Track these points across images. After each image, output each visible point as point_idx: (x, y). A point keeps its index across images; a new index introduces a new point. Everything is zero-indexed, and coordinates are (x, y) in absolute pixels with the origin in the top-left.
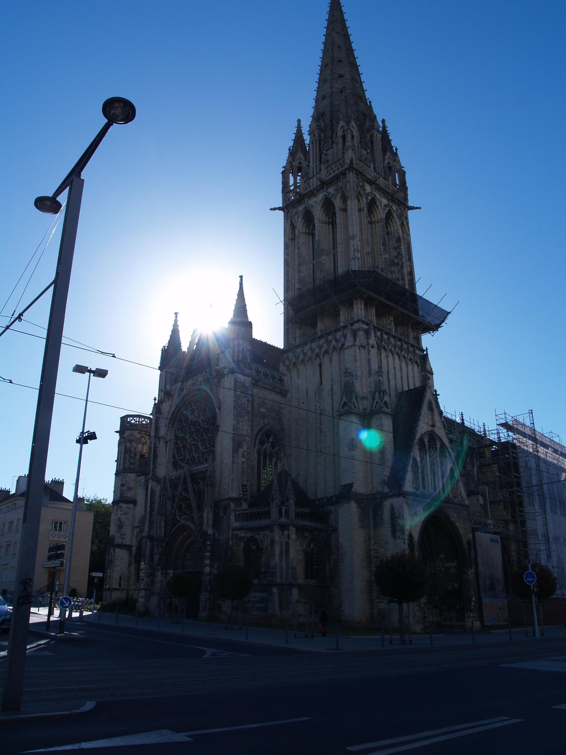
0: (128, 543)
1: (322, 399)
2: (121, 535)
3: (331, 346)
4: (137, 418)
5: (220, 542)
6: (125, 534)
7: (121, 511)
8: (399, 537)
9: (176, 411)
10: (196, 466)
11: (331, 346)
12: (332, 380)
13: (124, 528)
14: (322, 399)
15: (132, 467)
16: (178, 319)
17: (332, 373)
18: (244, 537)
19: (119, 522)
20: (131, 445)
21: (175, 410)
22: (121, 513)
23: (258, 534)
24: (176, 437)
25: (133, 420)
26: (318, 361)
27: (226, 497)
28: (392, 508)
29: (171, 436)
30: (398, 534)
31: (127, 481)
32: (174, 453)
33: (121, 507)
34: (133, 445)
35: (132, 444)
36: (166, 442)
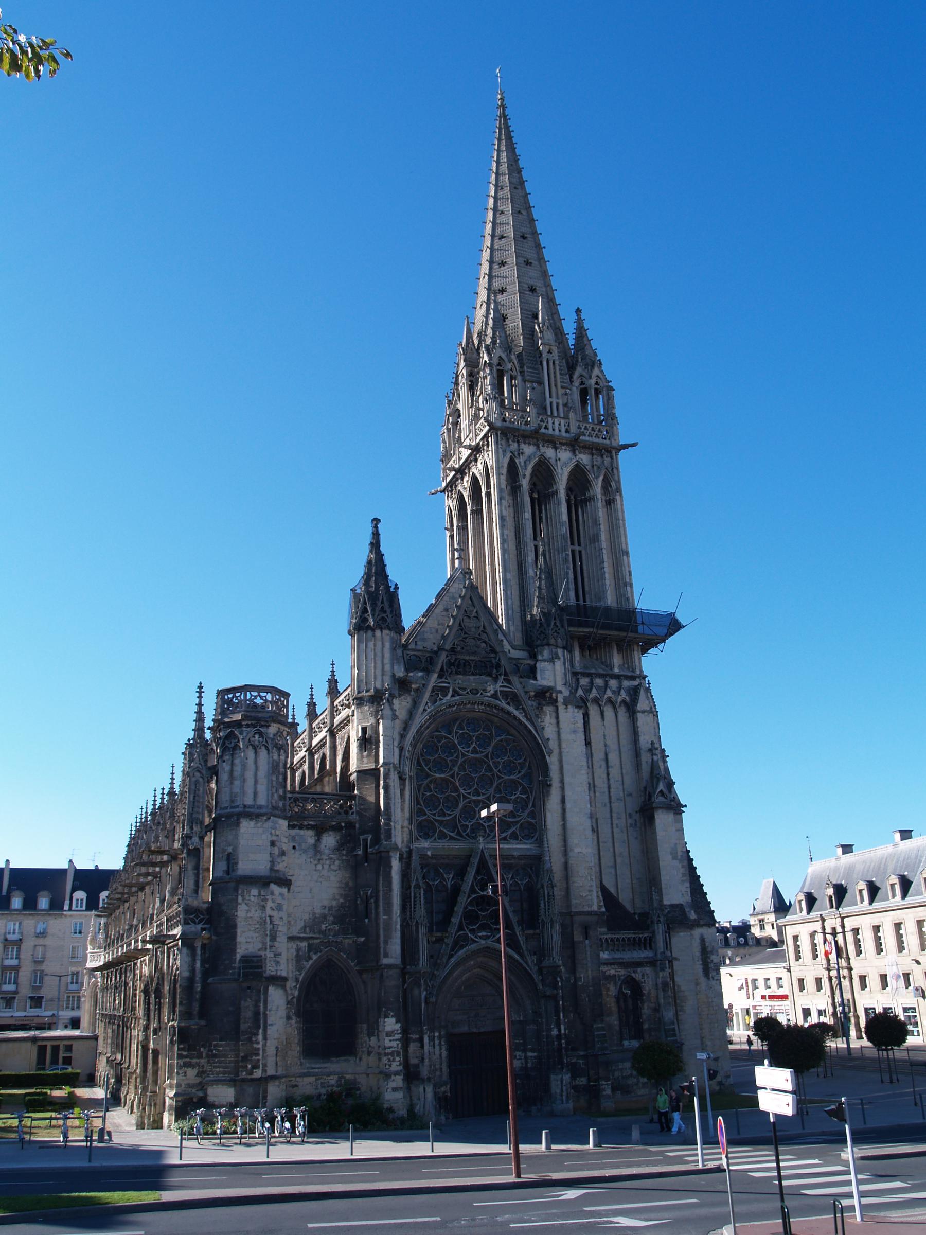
0: (284, 974)
5: (580, 983)
7: (273, 901)
8: (713, 978)
11: (606, 696)
12: (606, 745)
16: (380, 531)
17: (604, 736)
18: (615, 976)
23: (634, 972)
24: (421, 774)
27: (587, 909)
28: (703, 940)
30: (713, 974)
32: (418, 803)
33: (272, 893)
36: (402, 779)
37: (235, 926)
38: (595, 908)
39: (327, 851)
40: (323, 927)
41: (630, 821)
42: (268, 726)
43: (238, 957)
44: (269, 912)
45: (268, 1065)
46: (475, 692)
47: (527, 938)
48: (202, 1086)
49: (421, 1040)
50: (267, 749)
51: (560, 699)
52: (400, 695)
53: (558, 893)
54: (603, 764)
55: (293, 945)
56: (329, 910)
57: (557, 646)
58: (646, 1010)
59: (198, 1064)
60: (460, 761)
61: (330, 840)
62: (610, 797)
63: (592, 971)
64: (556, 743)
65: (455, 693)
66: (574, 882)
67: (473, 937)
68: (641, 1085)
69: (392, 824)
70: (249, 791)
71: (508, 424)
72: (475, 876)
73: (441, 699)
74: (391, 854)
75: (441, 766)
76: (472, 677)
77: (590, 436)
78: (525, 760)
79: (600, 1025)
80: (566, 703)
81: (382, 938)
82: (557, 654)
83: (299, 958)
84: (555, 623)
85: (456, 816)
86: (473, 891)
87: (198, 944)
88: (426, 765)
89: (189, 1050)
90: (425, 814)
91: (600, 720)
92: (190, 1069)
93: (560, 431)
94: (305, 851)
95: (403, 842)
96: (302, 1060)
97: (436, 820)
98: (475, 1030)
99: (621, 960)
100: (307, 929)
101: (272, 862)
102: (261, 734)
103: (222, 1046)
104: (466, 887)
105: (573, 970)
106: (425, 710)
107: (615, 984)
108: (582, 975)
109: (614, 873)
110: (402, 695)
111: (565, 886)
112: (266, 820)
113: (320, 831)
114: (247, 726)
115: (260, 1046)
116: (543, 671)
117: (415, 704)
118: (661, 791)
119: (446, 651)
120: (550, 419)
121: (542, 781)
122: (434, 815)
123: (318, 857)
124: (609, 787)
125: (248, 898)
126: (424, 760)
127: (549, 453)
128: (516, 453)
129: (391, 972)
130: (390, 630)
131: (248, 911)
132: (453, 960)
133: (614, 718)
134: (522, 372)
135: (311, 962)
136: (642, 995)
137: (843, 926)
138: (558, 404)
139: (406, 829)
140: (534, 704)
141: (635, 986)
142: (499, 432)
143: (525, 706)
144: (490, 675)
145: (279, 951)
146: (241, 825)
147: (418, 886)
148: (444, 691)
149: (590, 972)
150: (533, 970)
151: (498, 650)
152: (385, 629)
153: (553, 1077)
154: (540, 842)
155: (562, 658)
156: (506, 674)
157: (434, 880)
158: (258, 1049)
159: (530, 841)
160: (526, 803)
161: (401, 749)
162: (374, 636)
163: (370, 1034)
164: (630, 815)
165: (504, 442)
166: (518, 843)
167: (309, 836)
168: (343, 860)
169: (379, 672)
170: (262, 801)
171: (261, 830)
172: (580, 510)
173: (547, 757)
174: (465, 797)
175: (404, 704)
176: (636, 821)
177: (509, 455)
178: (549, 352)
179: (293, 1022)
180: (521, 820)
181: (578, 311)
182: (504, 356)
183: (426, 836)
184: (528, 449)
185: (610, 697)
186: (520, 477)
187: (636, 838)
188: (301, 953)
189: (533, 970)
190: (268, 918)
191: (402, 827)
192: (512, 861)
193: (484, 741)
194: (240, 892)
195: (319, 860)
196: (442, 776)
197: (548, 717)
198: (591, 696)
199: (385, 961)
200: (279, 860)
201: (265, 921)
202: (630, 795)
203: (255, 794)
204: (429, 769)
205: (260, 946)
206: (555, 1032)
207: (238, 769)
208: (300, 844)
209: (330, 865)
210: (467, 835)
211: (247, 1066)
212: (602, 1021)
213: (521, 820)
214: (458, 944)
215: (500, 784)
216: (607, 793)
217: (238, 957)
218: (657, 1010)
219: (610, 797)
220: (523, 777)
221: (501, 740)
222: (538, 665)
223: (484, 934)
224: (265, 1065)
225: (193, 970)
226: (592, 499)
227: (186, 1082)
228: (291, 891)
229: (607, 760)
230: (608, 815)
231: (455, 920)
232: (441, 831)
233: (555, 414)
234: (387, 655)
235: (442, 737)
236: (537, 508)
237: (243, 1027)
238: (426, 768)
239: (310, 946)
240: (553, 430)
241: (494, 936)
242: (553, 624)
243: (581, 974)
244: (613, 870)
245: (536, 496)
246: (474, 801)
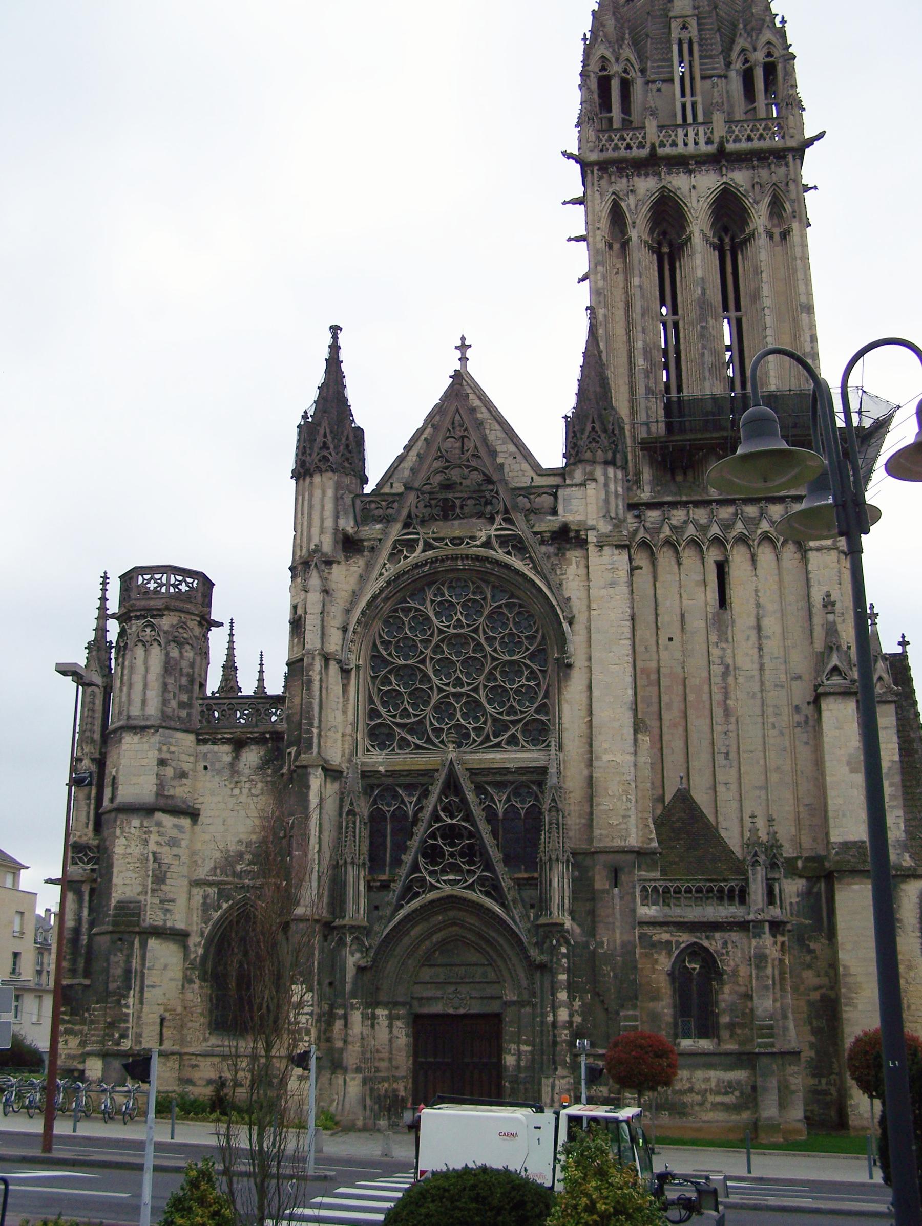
0: (180, 925)
1: (727, 641)
2: (162, 902)
3: (759, 531)
4: (194, 579)
6: (173, 901)
7: (160, 834)
9: (383, 596)
10: (471, 752)
12: (758, 605)
13: (168, 881)
14: (727, 641)
15: (183, 713)
16: (341, 342)
17: (756, 591)
18: (669, 943)
19: (156, 865)
20: (180, 652)
21: (382, 591)
22: (160, 839)
23: (707, 938)
24: (377, 660)
25: (184, 584)
26: (713, 555)
27: (618, 843)
29: (358, 658)
31: (173, 752)
33: (159, 824)
34: (186, 654)
35: (183, 650)
36: (345, 672)
38: (633, 841)
39: (247, 772)
40: (238, 868)
41: (797, 718)
42: (162, 616)
43: (113, 902)
44: (152, 847)
45: (144, 1035)
46: (457, 541)
47: (521, 884)
48: (84, 1057)
49: (345, 1017)
50: (160, 645)
51: (592, 537)
52: (347, 559)
53: (574, 819)
54: (753, 634)
55: (198, 894)
56: (246, 847)
57: (593, 462)
58: (727, 995)
59: (81, 1032)
60: (435, 640)
61: (252, 757)
62: (762, 683)
63: (621, 933)
64: (585, 602)
65: (428, 546)
66: (598, 804)
67: (433, 882)
68: (709, 1106)
69: (315, 731)
70: (137, 697)
71: (610, 154)
72: (440, 799)
73: (406, 557)
74: (310, 770)
75: (407, 647)
76: (456, 523)
77: (749, 139)
78: (537, 631)
79: (630, 1012)
80: (600, 547)
82: (592, 473)
84: (593, 428)
85: (425, 717)
86: (436, 818)
87: (86, 889)
88: (386, 650)
89: (71, 1014)
90: (379, 715)
91: (750, 568)
92: (71, 1037)
93: (696, 144)
94: (219, 772)
95: (343, 756)
96: (207, 1035)
97: (397, 725)
98: (451, 1011)
99: (679, 919)
100: (218, 871)
101: (161, 786)
102: (152, 626)
104: (426, 814)
105: (591, 932)
106: (381, 574)
107: (670, 953)
108: (605, 939)
109: (764, 797)
110: (351, 558)
111: (588, 810)
112: (153, 734)
113: (239, 745)
114: (137, 618)
115: (130, 1011)
116: (567, 500)
117: (369, 566)
118: (835, 669)
119: (417, 490)
120: (680, 132)
121: (557, 659)
122: (394, 716)
123: (236, 779)
124: (762, 668)
125: (127, 830)
126: (382, 643)
127: (679, 182)
128: (621, 195)
129: (301, 925)
130: (333, 471)
131: (127, 846)
132: (402, 913)
133: (774, 564)
134: (643, 71)
135: (219, 913)
136: (720, 974)
138: (694, 104)
139: (348, 738)
140: (551, 549)
141: (709, 960)
142: (596, 168)
143: (533, 554)
144: (480, 515)
145: (170, 896)
146: (123, 741)
147: (351, 812)
148: (411, 545)
149: (618, 935)
150: (521, 928)
151: (495, 477)
152: (327, 471)
153: (544, 1080)
155: (601, 479)
156: (506, 511)
157: (389, 805)
158: (127, 1015)
159: (538, 748)
160: (536, 693)
161: (345, 630)
162: (311, 483)
164: (797, 709)
165: (604, 182)
166: (518, 751)
167: (224, 752)
168: (267, 782)
169: (315, 531)
170: (153, 708)
171: (146, 746)
172: (740, 257)
173: (565, 626)
174: (440, 690)
175: (354, 569)
176: (807, 717)
177: (609, 198)
179: (196, 986)
180: (525, 717)
182: (608, 54)
183: (382, 746)
185: (767, 532)
186: (629, 226)
187: (807, 743)
188: (208, 901)
190: (151, 855)
191: (343, 735)
192: (510, 777)
194: (118, 823)
195: (237, 782)
196: (409, 662)
197: (574, 566)
198: (734, 533)
200: (175, 783)
201: (147, 859)
202: (799, 677)
203: (144, 702)
204: (390, 654)
205: (140, 889)
206: (550, 1018)
208: (213, 764)
209: (250, 789)
210: (442, 742)
211: (113, 1035)
212: (635, 1007)
213: (525, 717)
214: (409, 893)
215: (495, 668)
216: (757, 678)
217: (113, 902)
218: (748, 997)
219: (762, 683)
220: (532, 657)
221: (500, 607)
222: (561, 493)
223: (451, 877)
224: (139, 1035)
225: (79, 920)
227: (66, 1052)
228: (200, 822)
229: (759, 628)
230: (758, 711)
231: (408, 858)
232: (402, 739)
233: (690, 119)
234: (329, 506)
235: (409, 609)
236: (667, 267)
237: (112, 986)
238: (384, 653)
239: (220, 893)
240: (686, 144)
241: (466, 881)
242: (588, 428)
244: (763, 793)
245: (665, 250)
246: (455, 695)
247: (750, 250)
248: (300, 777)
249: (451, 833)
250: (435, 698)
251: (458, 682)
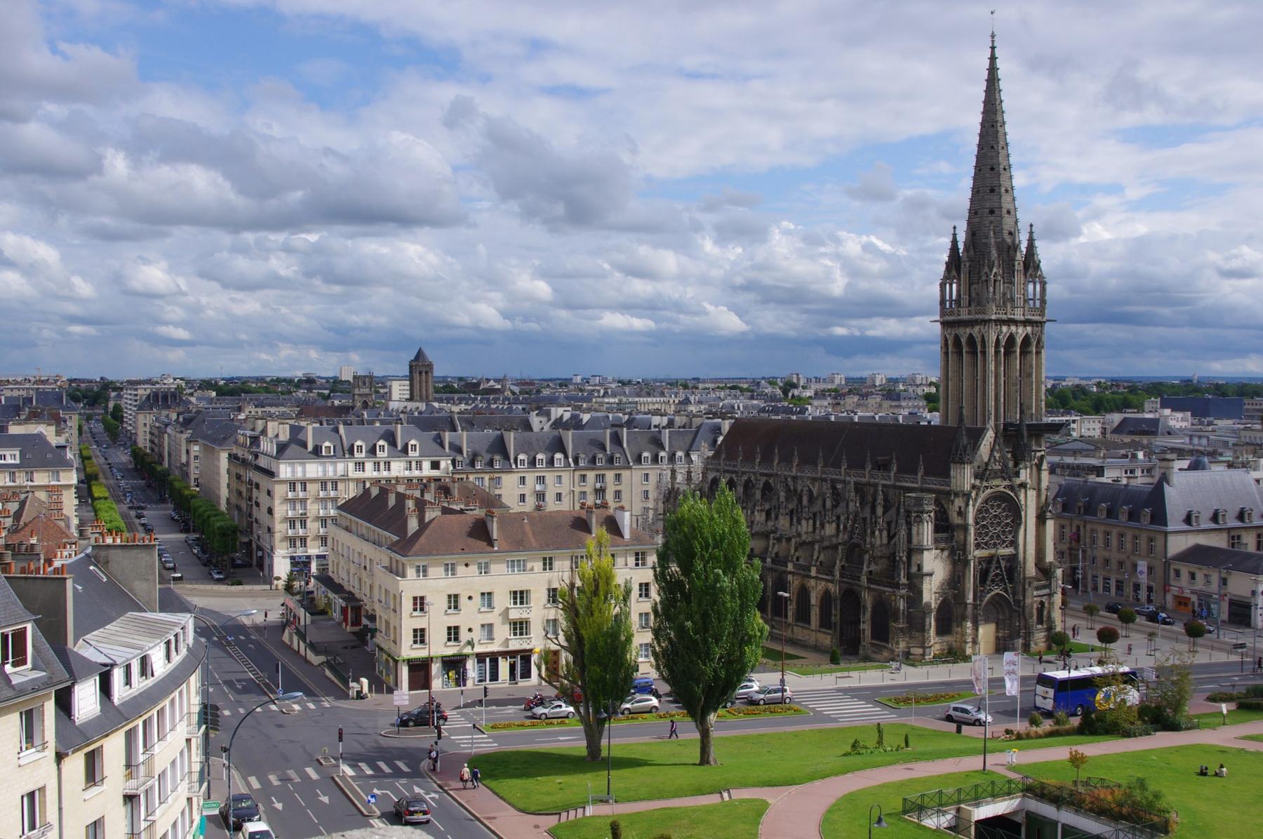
24: (977, 523)
37: (922, 591)
46: (998, 486)
48: (909, 648)
61: (946, 553)
65: (991, 488)
75: (984, 518)
81: (967, 590)
83: (936, 600)
103: (917, 634)
113: (942, 550)
117: (977, 494)
132: (986, 599)
134: (1003, 278)
137: (1085, 527)
141: (1042, 603)
148: (987, 487)
150: (1011, 600)
154: (1016, 548)
163: (958, 627)
178: (1019, 264)
181: (1031, 226)
184: (1005, 329)
189: (1011, 600)
193: (999, 506)
199: (968, 601)
207: (921, 531)
218: (1049, 612)
226: (1031, 352)
243: (1027, 601)
247: (1028, 357)
248: (967, 563)
249: (997, 575)
250: (990, 534)
251: (995, 529)
